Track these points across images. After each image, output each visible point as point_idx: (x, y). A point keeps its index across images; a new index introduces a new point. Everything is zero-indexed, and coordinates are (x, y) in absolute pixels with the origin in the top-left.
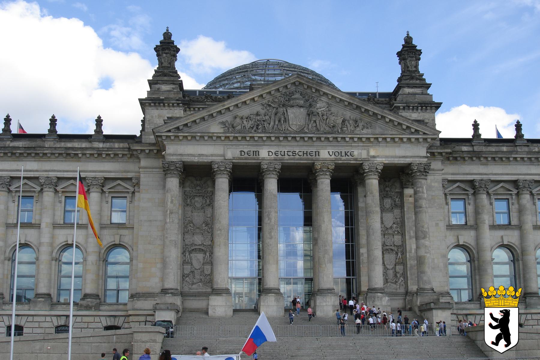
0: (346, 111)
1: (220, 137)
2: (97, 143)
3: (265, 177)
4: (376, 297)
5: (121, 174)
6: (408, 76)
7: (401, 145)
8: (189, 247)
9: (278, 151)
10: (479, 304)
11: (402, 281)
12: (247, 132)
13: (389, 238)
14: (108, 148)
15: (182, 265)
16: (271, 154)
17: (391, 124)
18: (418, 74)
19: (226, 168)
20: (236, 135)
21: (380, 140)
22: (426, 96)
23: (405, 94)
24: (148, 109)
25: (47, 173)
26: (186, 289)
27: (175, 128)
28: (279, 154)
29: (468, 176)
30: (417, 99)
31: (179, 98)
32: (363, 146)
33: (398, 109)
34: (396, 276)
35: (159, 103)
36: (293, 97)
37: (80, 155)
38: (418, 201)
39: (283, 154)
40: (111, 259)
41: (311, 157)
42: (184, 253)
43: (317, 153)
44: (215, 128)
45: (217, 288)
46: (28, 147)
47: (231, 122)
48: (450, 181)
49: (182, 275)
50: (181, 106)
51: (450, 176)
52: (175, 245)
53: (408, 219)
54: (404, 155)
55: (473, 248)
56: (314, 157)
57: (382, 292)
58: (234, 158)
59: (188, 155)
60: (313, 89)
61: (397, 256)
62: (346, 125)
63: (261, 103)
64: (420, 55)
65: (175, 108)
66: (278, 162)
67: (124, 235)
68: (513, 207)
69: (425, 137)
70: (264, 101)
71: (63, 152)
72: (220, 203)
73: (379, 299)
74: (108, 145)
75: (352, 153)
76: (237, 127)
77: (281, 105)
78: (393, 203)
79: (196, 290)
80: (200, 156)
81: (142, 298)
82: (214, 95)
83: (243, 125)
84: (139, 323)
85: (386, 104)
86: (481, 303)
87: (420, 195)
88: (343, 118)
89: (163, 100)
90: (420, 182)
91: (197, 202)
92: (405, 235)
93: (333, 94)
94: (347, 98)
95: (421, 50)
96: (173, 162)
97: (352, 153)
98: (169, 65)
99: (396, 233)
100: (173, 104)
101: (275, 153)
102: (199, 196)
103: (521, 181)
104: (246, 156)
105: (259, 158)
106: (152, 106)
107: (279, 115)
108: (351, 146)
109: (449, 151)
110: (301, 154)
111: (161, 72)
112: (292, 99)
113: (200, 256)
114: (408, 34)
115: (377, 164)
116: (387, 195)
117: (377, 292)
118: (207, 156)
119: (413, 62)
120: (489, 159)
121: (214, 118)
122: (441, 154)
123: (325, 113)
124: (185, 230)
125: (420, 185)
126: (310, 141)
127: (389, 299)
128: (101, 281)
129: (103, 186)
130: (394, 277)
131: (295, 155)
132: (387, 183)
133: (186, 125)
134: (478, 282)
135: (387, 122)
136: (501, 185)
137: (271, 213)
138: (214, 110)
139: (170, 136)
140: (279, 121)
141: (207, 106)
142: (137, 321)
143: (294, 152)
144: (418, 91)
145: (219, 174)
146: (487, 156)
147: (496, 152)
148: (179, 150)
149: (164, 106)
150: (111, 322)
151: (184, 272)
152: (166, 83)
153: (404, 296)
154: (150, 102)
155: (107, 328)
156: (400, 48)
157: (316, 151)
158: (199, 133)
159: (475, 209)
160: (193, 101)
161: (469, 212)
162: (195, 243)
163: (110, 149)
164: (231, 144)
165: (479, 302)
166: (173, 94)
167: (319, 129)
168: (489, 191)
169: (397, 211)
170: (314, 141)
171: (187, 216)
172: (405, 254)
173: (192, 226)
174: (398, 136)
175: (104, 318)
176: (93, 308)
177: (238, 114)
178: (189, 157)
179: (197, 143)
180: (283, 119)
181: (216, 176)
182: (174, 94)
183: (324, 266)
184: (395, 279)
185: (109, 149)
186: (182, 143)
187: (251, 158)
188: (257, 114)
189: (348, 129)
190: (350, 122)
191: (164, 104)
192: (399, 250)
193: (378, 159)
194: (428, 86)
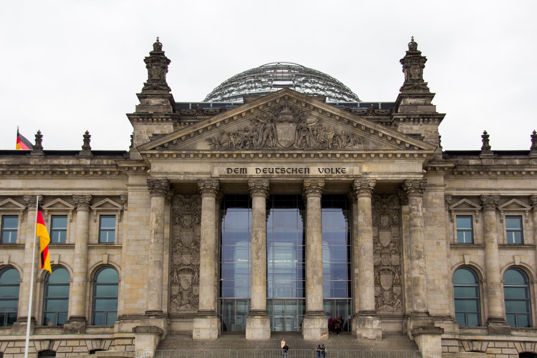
1: (206, 154)
2: (85, 160)
3: (253, 194)
4: (366, 320)
5: (109, 192)
6: (411, 85)
8: (177, 267)
10: (486, 329)
11: (399, 303)
12: (234, 149)
13: (386, 258)
14: (95, 165)
15: (170, 285)
16: (259, 171)
17: (384, 139)
18: (421, 83)
20: (223, 152)
21: (373, 156)
22: (429, 107)
24: (136, 124)
25: (32, 191)
26: (174, 311)
27: (160, 146)
28: (268, 171)
29: (475, 192)
30: (420, 110)
32: (355, 162)
33: (398, 121)
34: (393, 298)
35: (148, 118)
36: (282, 112)
37: (67, 173)
38: (413, 220)
39: (271, 171)
40: (99, 280)
42: (171, 274)
43: (307, 170)
44: (202, 146)
45: (202, 310)
46: (11, 165)
47: (218, 138)
48: (454, 197)
49: (169, 297)
50: (170, 121)
51: (455, 192)
52: (160, 266)
53: (406, 237)
54: (398, 171)
55: (482, 269)
56: (303, 174)
57: (373, 315)
58: (220, 175)
59: (174, 173)
62: (337, 141)
63: (249, 118)
64: (425, 62)
65: (164, 123)
67: (112, 255)
68: (527, 224)
69: (420, 152)
70: (252, 117)
71: (49, 170)
74: (96, 161)
75: (343, 170)
77: (269, 121)
78: (391, 220)
79: (184, 312)
81: (129, 321)
82: (206, 108)
83: (230, 141)
84: (125, 346)
85: (387, 115)
86: (488, 329)
87: (415, 213)
88: (334, 133)
89: (151, 115)
90: (415, 199)
91: (186, 220)
92: (403, 255)
93: (323, 109)
96: (158, 180)
97: (343, 170)
99: (394, 252)
100: (162, 119)
101: (263, 171)
102: (188, 214)
103: (535, 197)
104: (233, 173)
106: (141, 121)
108: (343, 162)
109: (452, 165)
110: (290, 171)
111: (150, 85)
112: (281, 114)
113: (189, 276)
114: (413, 40)
115: (369, 181)
117: (367, 314)
118: (193, 174)
119: (416, 71)
120: (499, 173)
122: (443, 168)
123: (316, 128)
124: (174, 249)
125: (414, 203)
126: (300, 158)
127: (379, 323)
128: (88, 303)
129: (91, 205)
131: (283, 172)
132: (384, 200)
133: (171, 142)
134: (486, 305)
136: (513, 200)
139: (154, 154)
141: (198, 121)
142: (122, 344)
143: (283, 169)
144: (421, 101)
145: (205, 192)
146: (496, 170)
147: (507, 166)
148: (164, 168)
149: (153, 121)
150: (97, 345)
151: (172, 292)
152: (155, 97)
154: (139, 117)
155: (92, 352)
156: (403, 55)
157: (305, 167)
158: (184, 150)
159: (483, 227)
160: (184, 115)
161: (477, 230)
162: (184, 263)
163: (98, 166)
164: (217, 161)
165: (486, 327)
167: (309, 145)
168: (499, 207)
169: (394, 229)
170: (303, 158)
171: (176, 235)
172: (402, 275)
173: (181, 245)
174: (392, 152)
175: (90, 341)
176: (79, 331)
178: (175, 176)
179: (183, 161)
180: (271, 135)
182: (163, 108)
183: (313, 287)
185: (96, 166)
187: (239, 175)
188: (246, 130)
189: (339, 144)
190: (342, 137)
191: (153, 119)
193: (371, 176)
194: (432, 96)
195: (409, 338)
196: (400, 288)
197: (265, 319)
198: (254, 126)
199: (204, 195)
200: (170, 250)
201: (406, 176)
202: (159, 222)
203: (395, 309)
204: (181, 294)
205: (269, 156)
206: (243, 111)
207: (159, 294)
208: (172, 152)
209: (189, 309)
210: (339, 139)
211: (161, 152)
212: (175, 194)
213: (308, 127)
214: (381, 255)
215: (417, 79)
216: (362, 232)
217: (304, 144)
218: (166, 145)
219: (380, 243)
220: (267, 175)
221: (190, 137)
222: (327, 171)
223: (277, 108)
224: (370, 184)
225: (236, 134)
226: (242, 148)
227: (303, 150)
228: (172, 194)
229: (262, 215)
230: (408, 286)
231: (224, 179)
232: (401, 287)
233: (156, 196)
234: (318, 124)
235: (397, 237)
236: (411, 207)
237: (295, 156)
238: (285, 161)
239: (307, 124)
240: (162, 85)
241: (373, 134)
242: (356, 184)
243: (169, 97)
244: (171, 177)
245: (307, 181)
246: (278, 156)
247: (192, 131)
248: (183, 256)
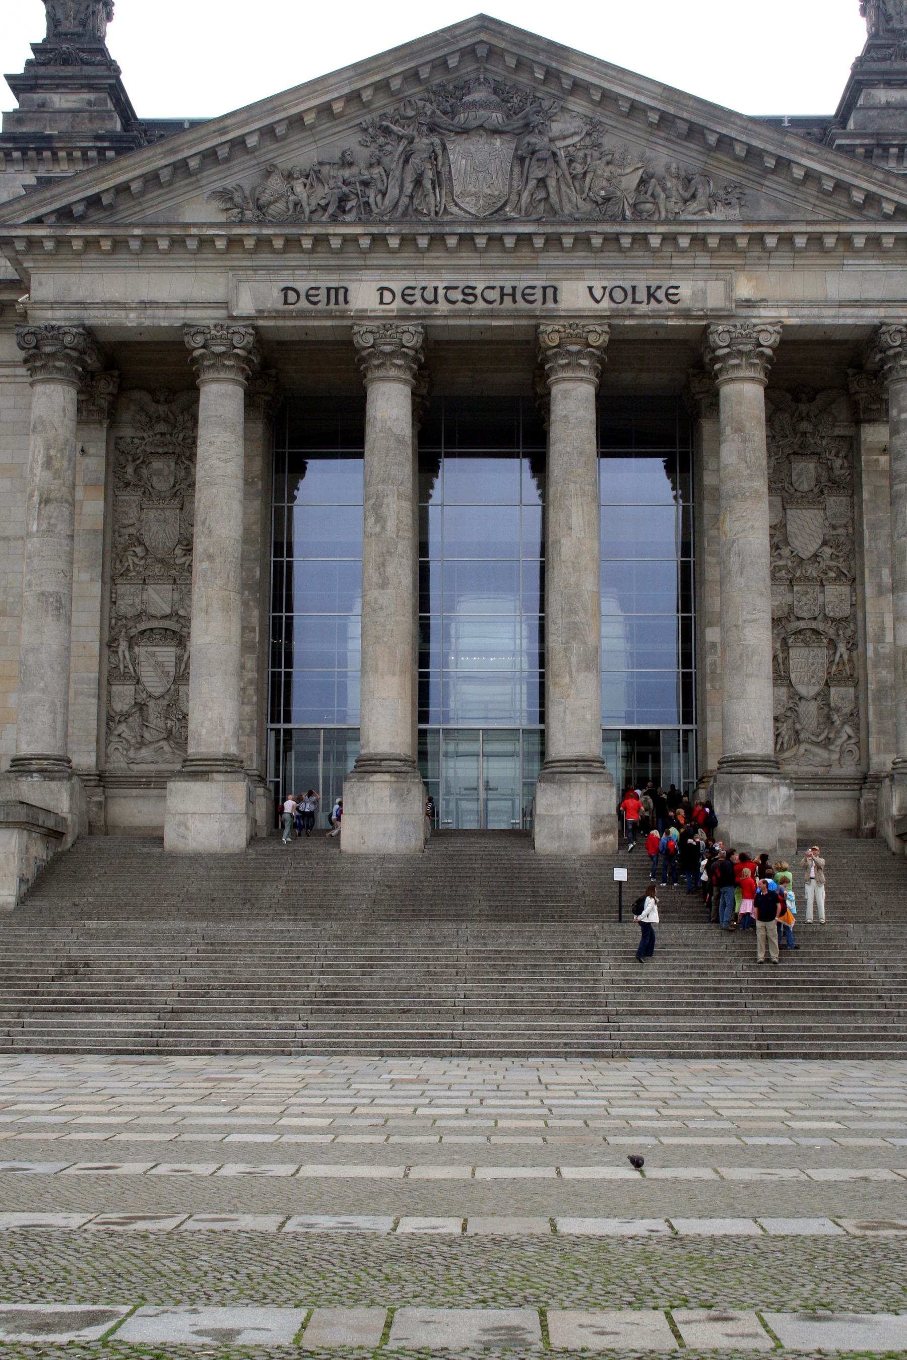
0: (653, 146)
3: (369, 375)
6: (889, 47)
7: (845, 262)
9: (413, 288)
11: (849, 737)
13: (807, 593)
15: (104, 682)
16: (388, 296)
17: (810, 190)
19: (235, 347)
20: (266, 231)
21: (771, 242)
23: (877, 108)
26: (118, 763)
28: (418, 297)
32: (711, 267)
35: (39, 151)
36: (466, 99)
39: (429, 295)
41: (529, 306)
42: (110, 644)
43: (550, 292)
45: (197, 753)
47: (253, 189)
52: (58, 609)
53: (873, 527)
54: (855, 296)
56: (538, 304)
57: (769, 770)
59: (106, 305)
60: (536, 70)
61: (835, 653)
62: (652, 195)
63: (357, 122)
66: (410, 326)
70: (368, 117)
72: (211, 467)
73: (755, 793)
75: (671, 291)
76: (272, 207)
77: (424, 128)
78: (824, 474)
79: (152, 767)
80: (145, 308)
83: (292, 198)
88: (641, 171)
89: (50, 138)
91: (159, 473)
92: (863, 584)
93: (606, 85)
94: (654, 98)
96: (53, 327)
97: (671, 291)
98: (81, 29)
101: (403, 295)
104: (303, 304)
105: (346, 311)
107: (416, 161)
108: (670, 266)
110: (493, 295)
111: (52, 50)
113: (167, 653)
115: (757, 328)
116: (803, 446)
118: (167, 306)
121: (194, 179)
123: (581, 154)
126: (525, 252)
127: (789, 797)
130: (825, 723)
131: (471, 298)
132: (803, 408)
133: (94, 201)
135: (794, 181)
137: (386, 501)
138: (189, 148)
140: (418, 183)
143: (470, 291)
145: (210, 367)
152: (65, 86)
153: (856, 787)
154: (10, 145)
158: (137, 225)
162: (152, 610)
164: (249, 264)
167: (557, 207)
169: (836, 503)
171: (126, 522)
174: (836, 229)
177: (277, 161)
178: (109, 313)
180: (429, 174)
181: (203, 377)
182: (91, 120)
183: (567, 680)
184: (826, 732)
186: (84, 264)
187: (320, 311)
190: (669, 184)
191: (54, 154)
192: (841, 632)
193: (763, 312)
195: (887, 846)
196: (852, 690)
197: (404, 785)
198: (373, 148)
199: (206, 376)
200: (108, 570)
201: (882, 312)
202: (57, 464)
203: (835, 756)
204: (141, 709)
205: (423, 242)
206: (336, 95)
207: (53, 703)
208: (96, 232)
209: (167, 756)
210: (659, 189)
211: (60, 232)
212: (121, 389)
213: (555, 150)
214: (791, 585)
216: (735, 496)
217: (542, 206)
218: (79, 209)
219: (788, 544)
220: (417, 310)
221: (160, 185)
222: (618, 295)
223: (451, 87)
224: (763, 338)
225: (313, 176)
227: (538, 221)
228: (112, 388)
229: (399, 440)
230: (879, 682)
231: (271, 323)
232: (856, 686)
233: (44, 381)
234: (588, 141)
235: (845, 526)
236: (899, 415)
237: (509, 242)
238: (478, 262)
239: (552, 140)
240: (90, 51)
241: (773, 171)
242: (714, 339)
243: (111, 86)
244: (96, 318)
246: (452, 242)
247: (164, 162)
248: (149, 588)
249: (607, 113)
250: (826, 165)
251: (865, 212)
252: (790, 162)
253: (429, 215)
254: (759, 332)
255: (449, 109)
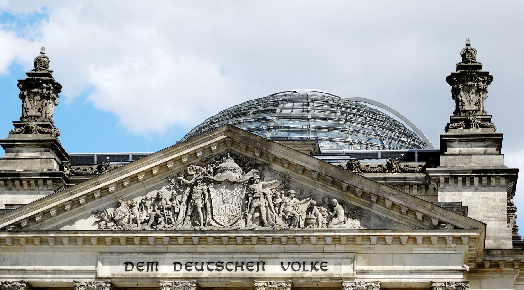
0: (316, 188)
6: (462, 120)
18: (480, 117)
30: (475, 163)
31: (49, 170)
35: (13, 181)
36: (221, 165)
63: (166, 177)
76: (122, 221)
83: (132, 216)
88: (309, 203)
89: (18, 174)
93: (290, 159)
95: (488, 73)
97: (324, 264)
100: (36, 181)
105: (156, 275)
131: (220, 268)
133: (32, 219)
143: (220, 264)
152: (29, 145)
157: (258, 260)
166: (38, 163)
180: (200, 205)
182: (41, 163)
187: (143, 275)
188: (158, 199)
193: (371, 276)
215: (473, 111)
220: (192, 274)
226: (152, 226)
245: (259, 285)
249: (292, 172)
250: (402, 200)
251: (424, 223)
252: (384, 198)
253: (200, 226)
254: (368, 286)
255: (212, 170)
